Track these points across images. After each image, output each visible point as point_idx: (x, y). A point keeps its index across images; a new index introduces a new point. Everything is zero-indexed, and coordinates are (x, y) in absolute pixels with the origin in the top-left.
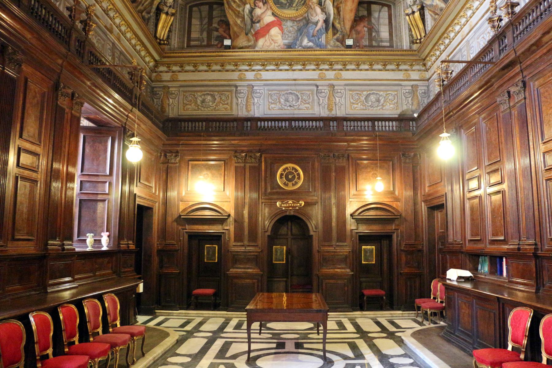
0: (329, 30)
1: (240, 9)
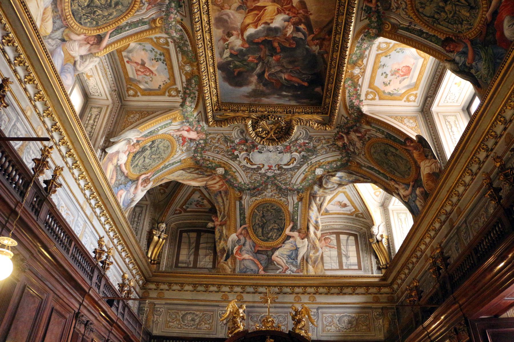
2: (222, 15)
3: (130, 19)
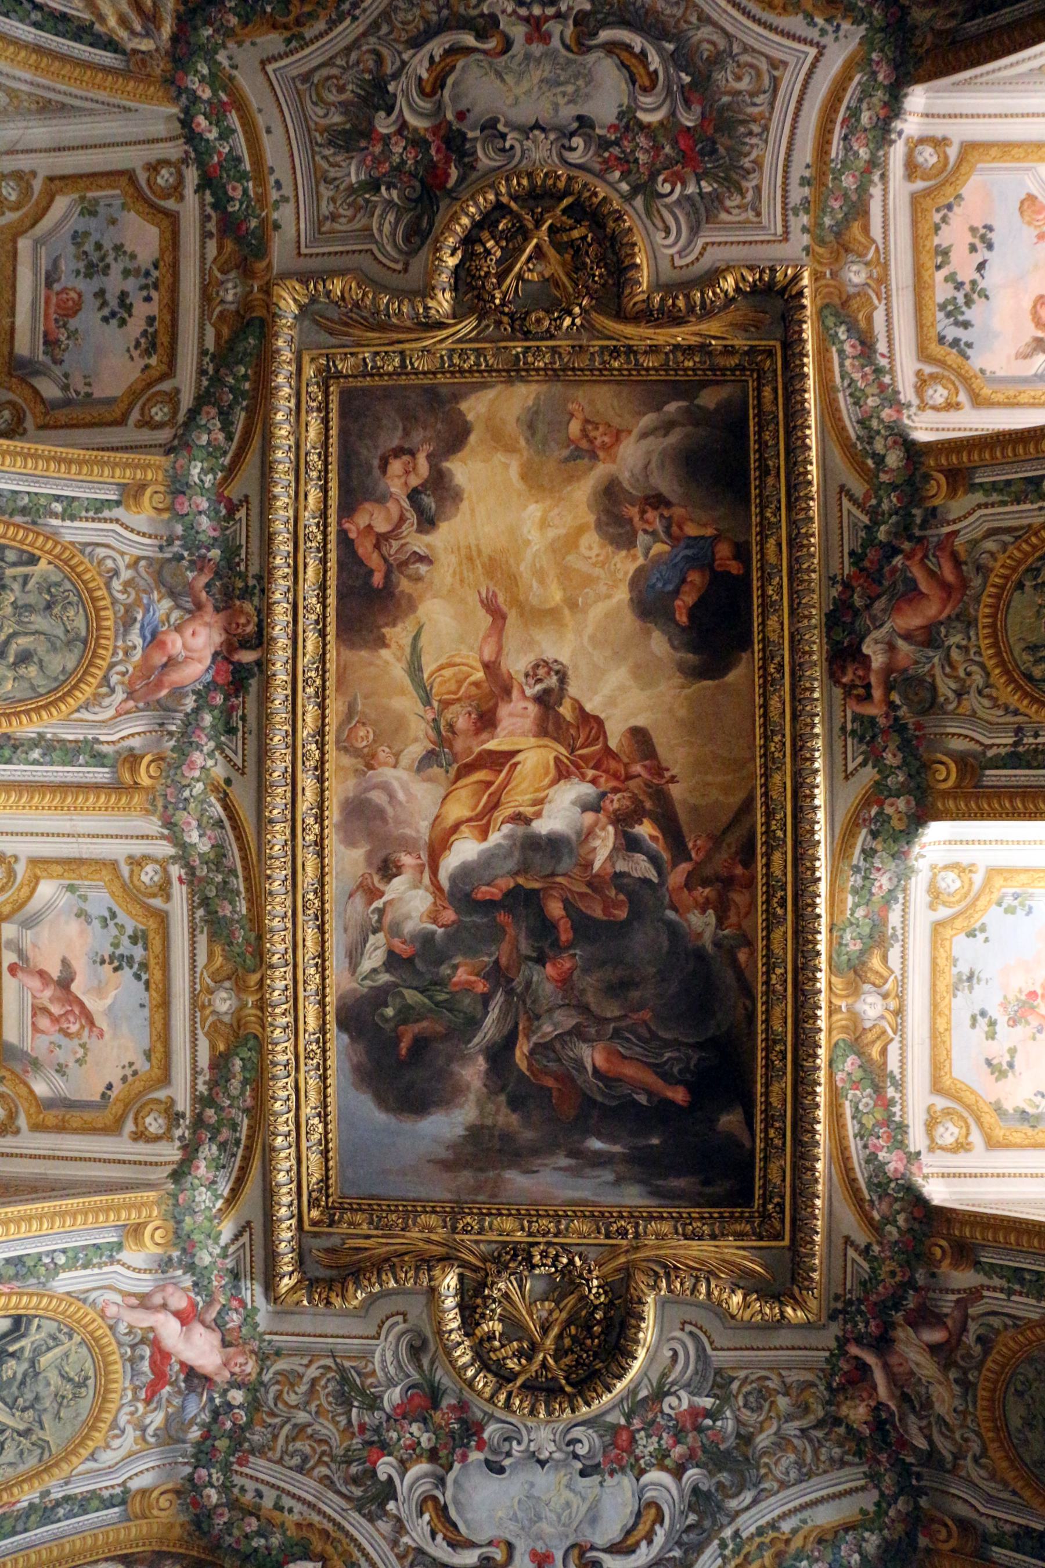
2: (367, 790)
3: (52, 726)
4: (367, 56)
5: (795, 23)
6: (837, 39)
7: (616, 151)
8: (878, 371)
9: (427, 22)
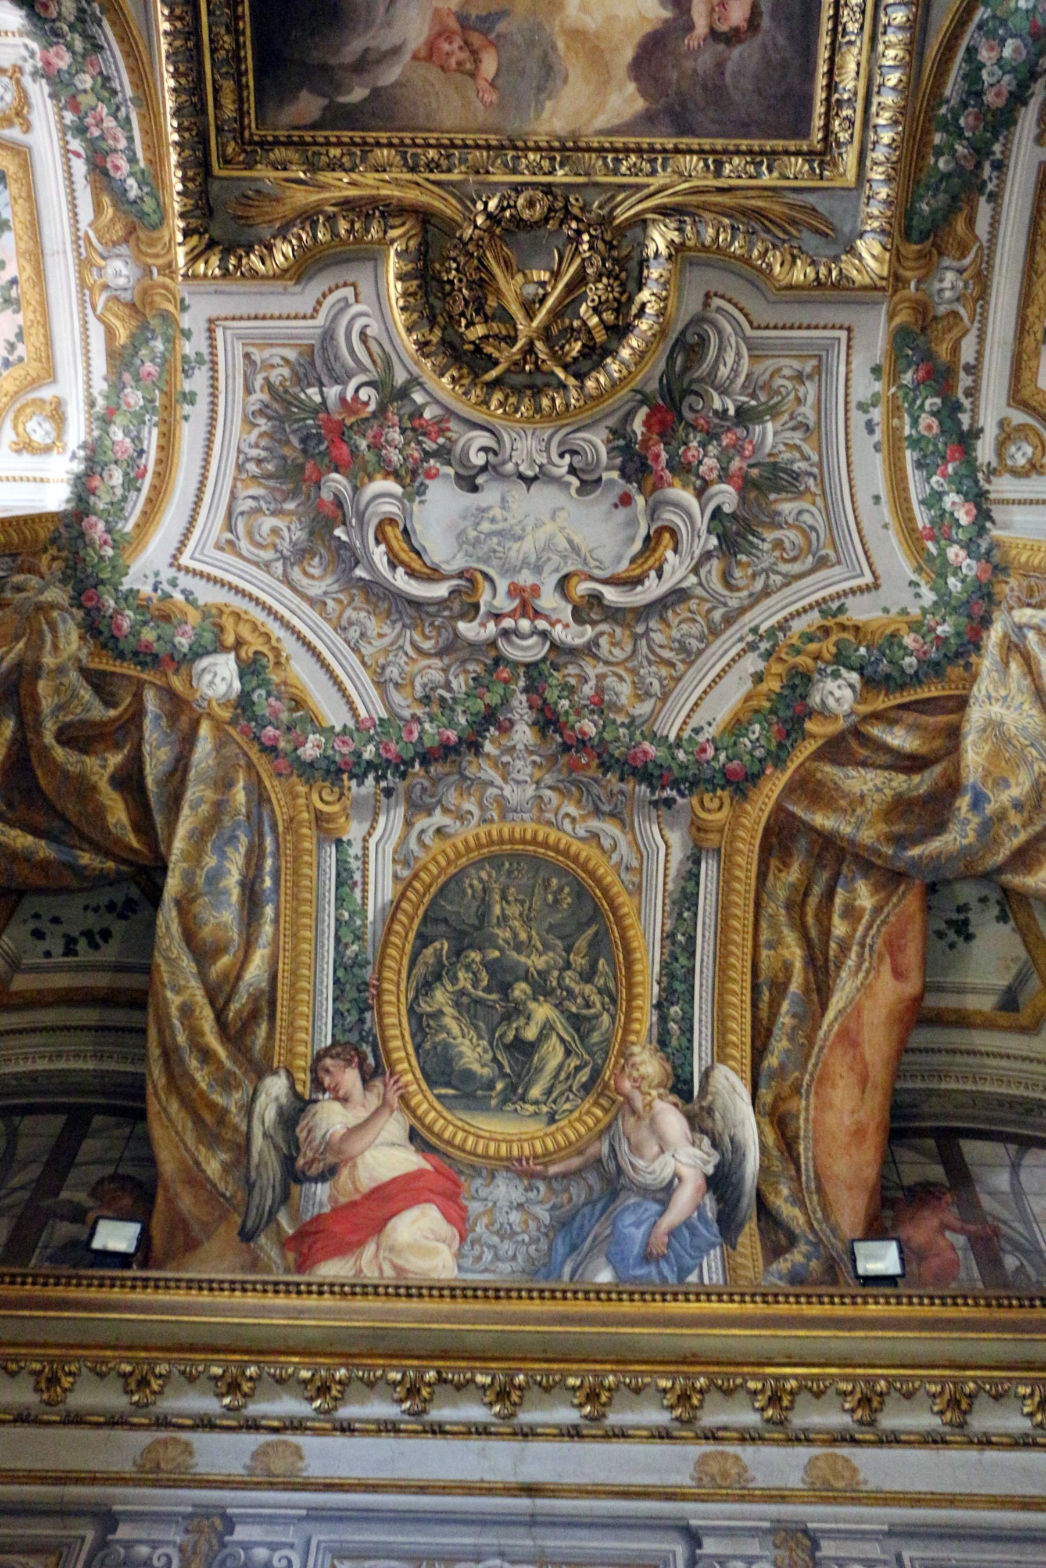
0: (741, 1226)
1: (232, 1102)
4: (741, 583)
5: (208, 595)
6: (157, 574)
7: (429, 445)
8: (81, 130)
9: (663, 620)
